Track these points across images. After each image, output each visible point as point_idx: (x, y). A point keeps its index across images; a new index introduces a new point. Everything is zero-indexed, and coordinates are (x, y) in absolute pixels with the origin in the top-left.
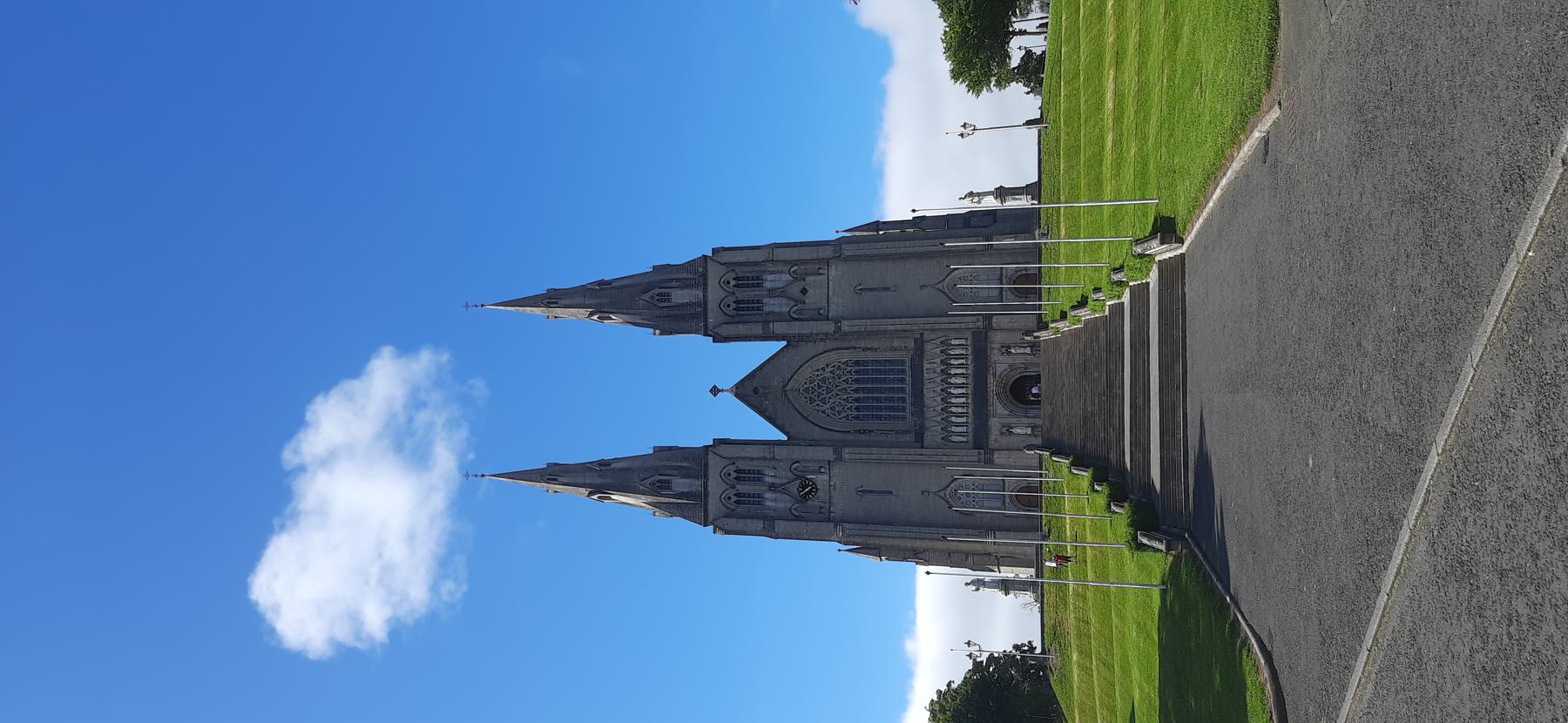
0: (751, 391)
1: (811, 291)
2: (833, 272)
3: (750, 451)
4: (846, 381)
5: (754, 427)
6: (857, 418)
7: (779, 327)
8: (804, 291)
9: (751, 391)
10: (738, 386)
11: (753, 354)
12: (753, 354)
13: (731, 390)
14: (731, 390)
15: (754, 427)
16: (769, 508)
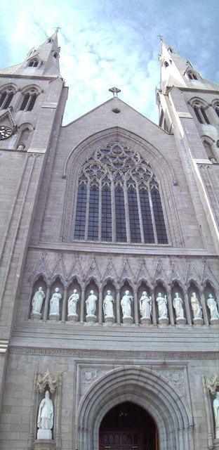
4: (130, 180)
6: (82, 188)
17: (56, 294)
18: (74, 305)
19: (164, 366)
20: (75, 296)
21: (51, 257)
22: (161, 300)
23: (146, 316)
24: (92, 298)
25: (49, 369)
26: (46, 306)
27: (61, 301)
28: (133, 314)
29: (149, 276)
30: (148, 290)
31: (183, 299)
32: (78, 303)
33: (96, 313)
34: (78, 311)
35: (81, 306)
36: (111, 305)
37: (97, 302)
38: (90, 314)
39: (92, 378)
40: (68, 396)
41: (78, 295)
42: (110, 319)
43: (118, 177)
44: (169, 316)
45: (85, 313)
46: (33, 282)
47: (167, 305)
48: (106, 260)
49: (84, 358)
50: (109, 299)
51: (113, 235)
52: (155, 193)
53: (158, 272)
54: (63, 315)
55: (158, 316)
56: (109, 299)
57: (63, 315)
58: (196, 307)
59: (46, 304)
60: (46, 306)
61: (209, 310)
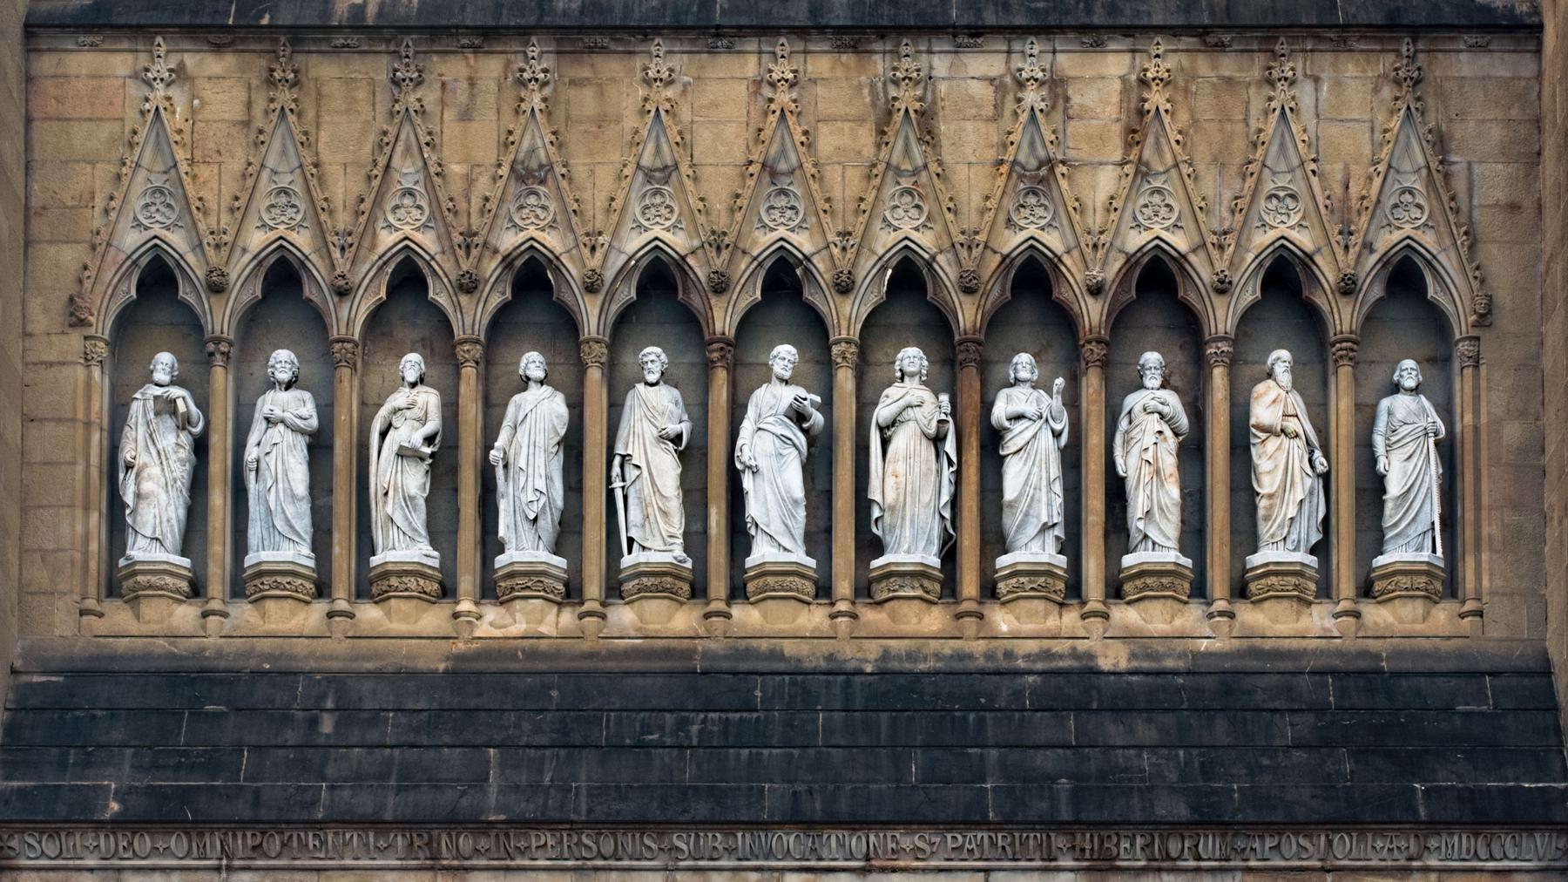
17: (275, 402)
18: (415, 480)
20: (412, 410)
23: (912, 546)
24: (538, 414)
26: (219, 499)
27: (319, 446)
28: (818, 537)
30: (938, 329)
31: (1197, 410)
32: (441, 460)
33: (567, 535)
34: (440, 530)
36: (666, 469)
37: (572, 446)
38: (525, 548)
41: (429, 398)
42: (659, 582)
44: (1071, 545)
45: (490, 543)
46: (103, 325)
47: (1072, 458)
55: (995, 540)
56: (655, 410)
58: (1284, 471)
60: (219, 499)
61: (1372, 487)
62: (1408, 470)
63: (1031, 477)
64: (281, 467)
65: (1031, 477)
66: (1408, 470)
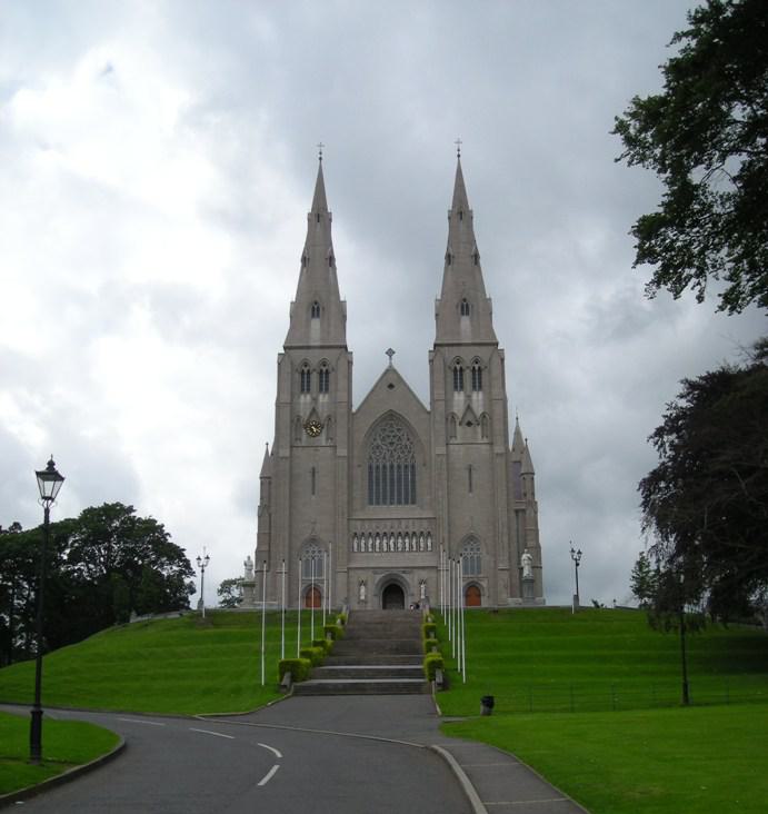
0: (391, 381)
1: (469, 429)
2: (484, 447)
3: (342, 383)
5: (362, 382)
6: (370, 467)
7: (441, 406)
8: (469, 424)
9: (391, 381)
10: (395, 371)
11: (419, 380)
12: (419, 380)
13: (391, 366)
14: (391, 366)
15: (362, 382)
16: (299, 397)
19: (404, 572)
20: (371, 542)
21: (359, 523)
22: (407, 541)
25: (363, 576)
29: (403, 530)
35: (374, 546)
39: (378, 577)
40: (370, 585)
43: (392, 456)
48: (383, 523)
49: (375, 570)
50: (385, 541)
51: (388, 501)
52: (413, 467)
53: (407, 527)
54: (367, 551)
56: (385, 541)
57: (367, 551)
59: (359, 546)
62: (429, 544)
63: (407, 545)
64: (363, 545)
65: (407, 545)
66: (429, 544)
